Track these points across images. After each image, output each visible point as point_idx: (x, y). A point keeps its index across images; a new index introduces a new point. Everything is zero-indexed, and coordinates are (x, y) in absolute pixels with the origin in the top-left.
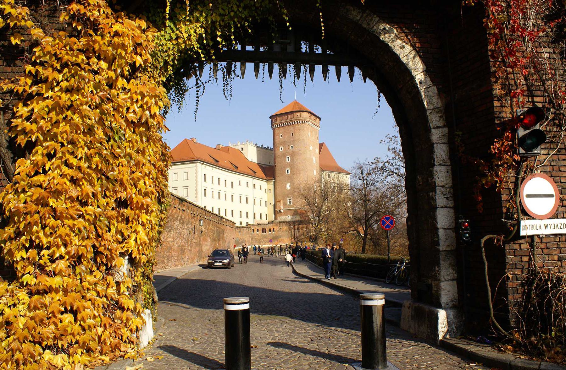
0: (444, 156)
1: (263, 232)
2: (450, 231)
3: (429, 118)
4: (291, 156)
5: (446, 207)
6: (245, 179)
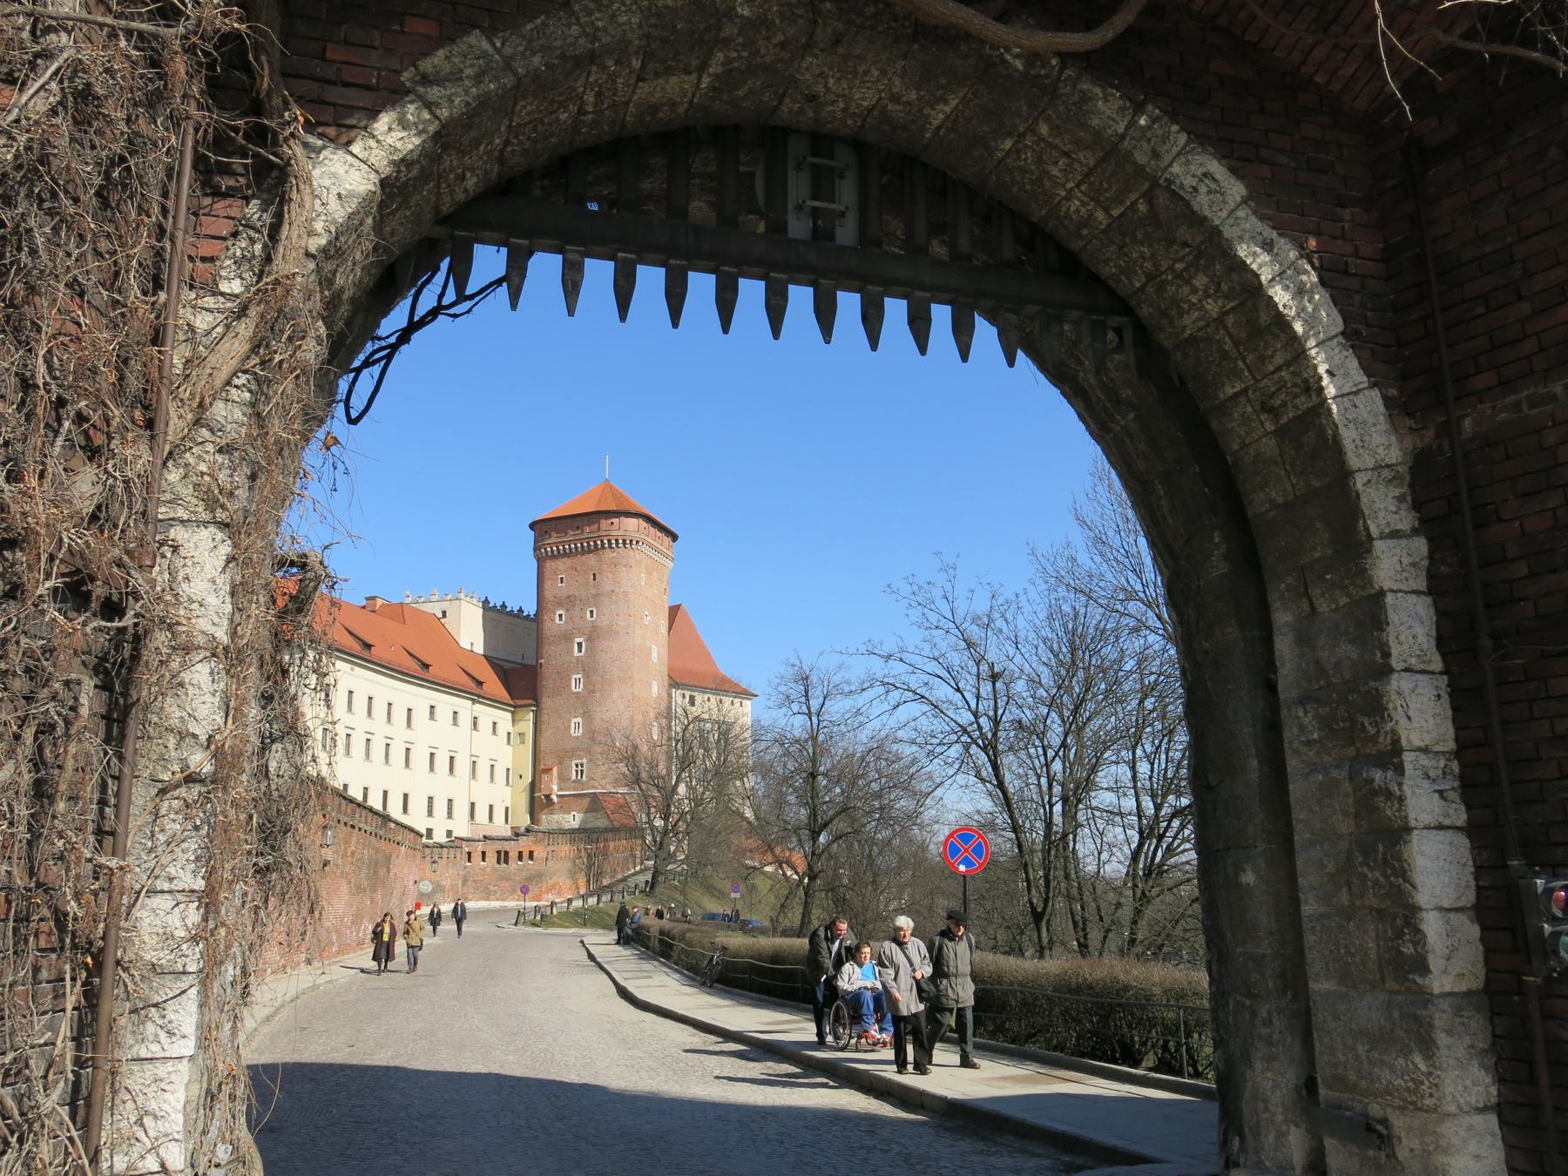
0: (1422, 639)
1: (499, 862)
2: (1462, 917)
3: (1364, 499)
4: (589, 640)
5: (1440, 827)
6: (447, 703)
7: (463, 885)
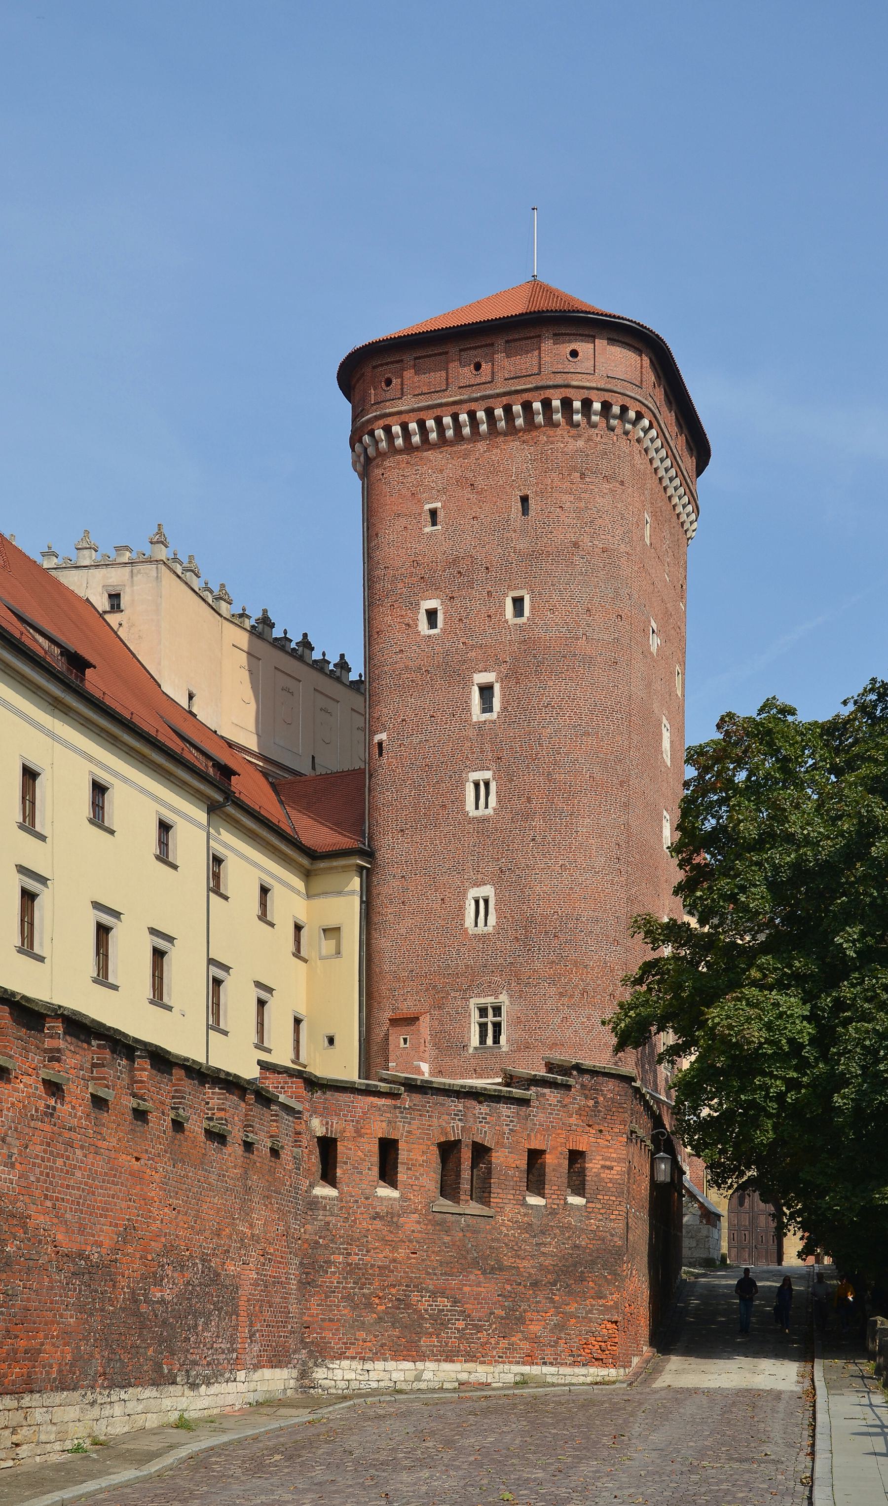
7: (306, 1284)
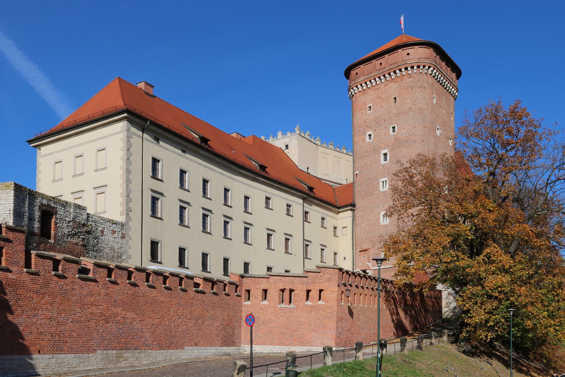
4: (392, 150)
